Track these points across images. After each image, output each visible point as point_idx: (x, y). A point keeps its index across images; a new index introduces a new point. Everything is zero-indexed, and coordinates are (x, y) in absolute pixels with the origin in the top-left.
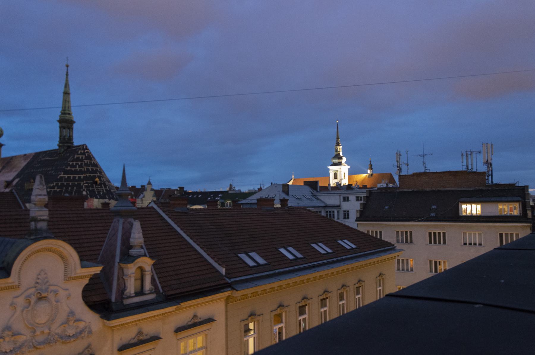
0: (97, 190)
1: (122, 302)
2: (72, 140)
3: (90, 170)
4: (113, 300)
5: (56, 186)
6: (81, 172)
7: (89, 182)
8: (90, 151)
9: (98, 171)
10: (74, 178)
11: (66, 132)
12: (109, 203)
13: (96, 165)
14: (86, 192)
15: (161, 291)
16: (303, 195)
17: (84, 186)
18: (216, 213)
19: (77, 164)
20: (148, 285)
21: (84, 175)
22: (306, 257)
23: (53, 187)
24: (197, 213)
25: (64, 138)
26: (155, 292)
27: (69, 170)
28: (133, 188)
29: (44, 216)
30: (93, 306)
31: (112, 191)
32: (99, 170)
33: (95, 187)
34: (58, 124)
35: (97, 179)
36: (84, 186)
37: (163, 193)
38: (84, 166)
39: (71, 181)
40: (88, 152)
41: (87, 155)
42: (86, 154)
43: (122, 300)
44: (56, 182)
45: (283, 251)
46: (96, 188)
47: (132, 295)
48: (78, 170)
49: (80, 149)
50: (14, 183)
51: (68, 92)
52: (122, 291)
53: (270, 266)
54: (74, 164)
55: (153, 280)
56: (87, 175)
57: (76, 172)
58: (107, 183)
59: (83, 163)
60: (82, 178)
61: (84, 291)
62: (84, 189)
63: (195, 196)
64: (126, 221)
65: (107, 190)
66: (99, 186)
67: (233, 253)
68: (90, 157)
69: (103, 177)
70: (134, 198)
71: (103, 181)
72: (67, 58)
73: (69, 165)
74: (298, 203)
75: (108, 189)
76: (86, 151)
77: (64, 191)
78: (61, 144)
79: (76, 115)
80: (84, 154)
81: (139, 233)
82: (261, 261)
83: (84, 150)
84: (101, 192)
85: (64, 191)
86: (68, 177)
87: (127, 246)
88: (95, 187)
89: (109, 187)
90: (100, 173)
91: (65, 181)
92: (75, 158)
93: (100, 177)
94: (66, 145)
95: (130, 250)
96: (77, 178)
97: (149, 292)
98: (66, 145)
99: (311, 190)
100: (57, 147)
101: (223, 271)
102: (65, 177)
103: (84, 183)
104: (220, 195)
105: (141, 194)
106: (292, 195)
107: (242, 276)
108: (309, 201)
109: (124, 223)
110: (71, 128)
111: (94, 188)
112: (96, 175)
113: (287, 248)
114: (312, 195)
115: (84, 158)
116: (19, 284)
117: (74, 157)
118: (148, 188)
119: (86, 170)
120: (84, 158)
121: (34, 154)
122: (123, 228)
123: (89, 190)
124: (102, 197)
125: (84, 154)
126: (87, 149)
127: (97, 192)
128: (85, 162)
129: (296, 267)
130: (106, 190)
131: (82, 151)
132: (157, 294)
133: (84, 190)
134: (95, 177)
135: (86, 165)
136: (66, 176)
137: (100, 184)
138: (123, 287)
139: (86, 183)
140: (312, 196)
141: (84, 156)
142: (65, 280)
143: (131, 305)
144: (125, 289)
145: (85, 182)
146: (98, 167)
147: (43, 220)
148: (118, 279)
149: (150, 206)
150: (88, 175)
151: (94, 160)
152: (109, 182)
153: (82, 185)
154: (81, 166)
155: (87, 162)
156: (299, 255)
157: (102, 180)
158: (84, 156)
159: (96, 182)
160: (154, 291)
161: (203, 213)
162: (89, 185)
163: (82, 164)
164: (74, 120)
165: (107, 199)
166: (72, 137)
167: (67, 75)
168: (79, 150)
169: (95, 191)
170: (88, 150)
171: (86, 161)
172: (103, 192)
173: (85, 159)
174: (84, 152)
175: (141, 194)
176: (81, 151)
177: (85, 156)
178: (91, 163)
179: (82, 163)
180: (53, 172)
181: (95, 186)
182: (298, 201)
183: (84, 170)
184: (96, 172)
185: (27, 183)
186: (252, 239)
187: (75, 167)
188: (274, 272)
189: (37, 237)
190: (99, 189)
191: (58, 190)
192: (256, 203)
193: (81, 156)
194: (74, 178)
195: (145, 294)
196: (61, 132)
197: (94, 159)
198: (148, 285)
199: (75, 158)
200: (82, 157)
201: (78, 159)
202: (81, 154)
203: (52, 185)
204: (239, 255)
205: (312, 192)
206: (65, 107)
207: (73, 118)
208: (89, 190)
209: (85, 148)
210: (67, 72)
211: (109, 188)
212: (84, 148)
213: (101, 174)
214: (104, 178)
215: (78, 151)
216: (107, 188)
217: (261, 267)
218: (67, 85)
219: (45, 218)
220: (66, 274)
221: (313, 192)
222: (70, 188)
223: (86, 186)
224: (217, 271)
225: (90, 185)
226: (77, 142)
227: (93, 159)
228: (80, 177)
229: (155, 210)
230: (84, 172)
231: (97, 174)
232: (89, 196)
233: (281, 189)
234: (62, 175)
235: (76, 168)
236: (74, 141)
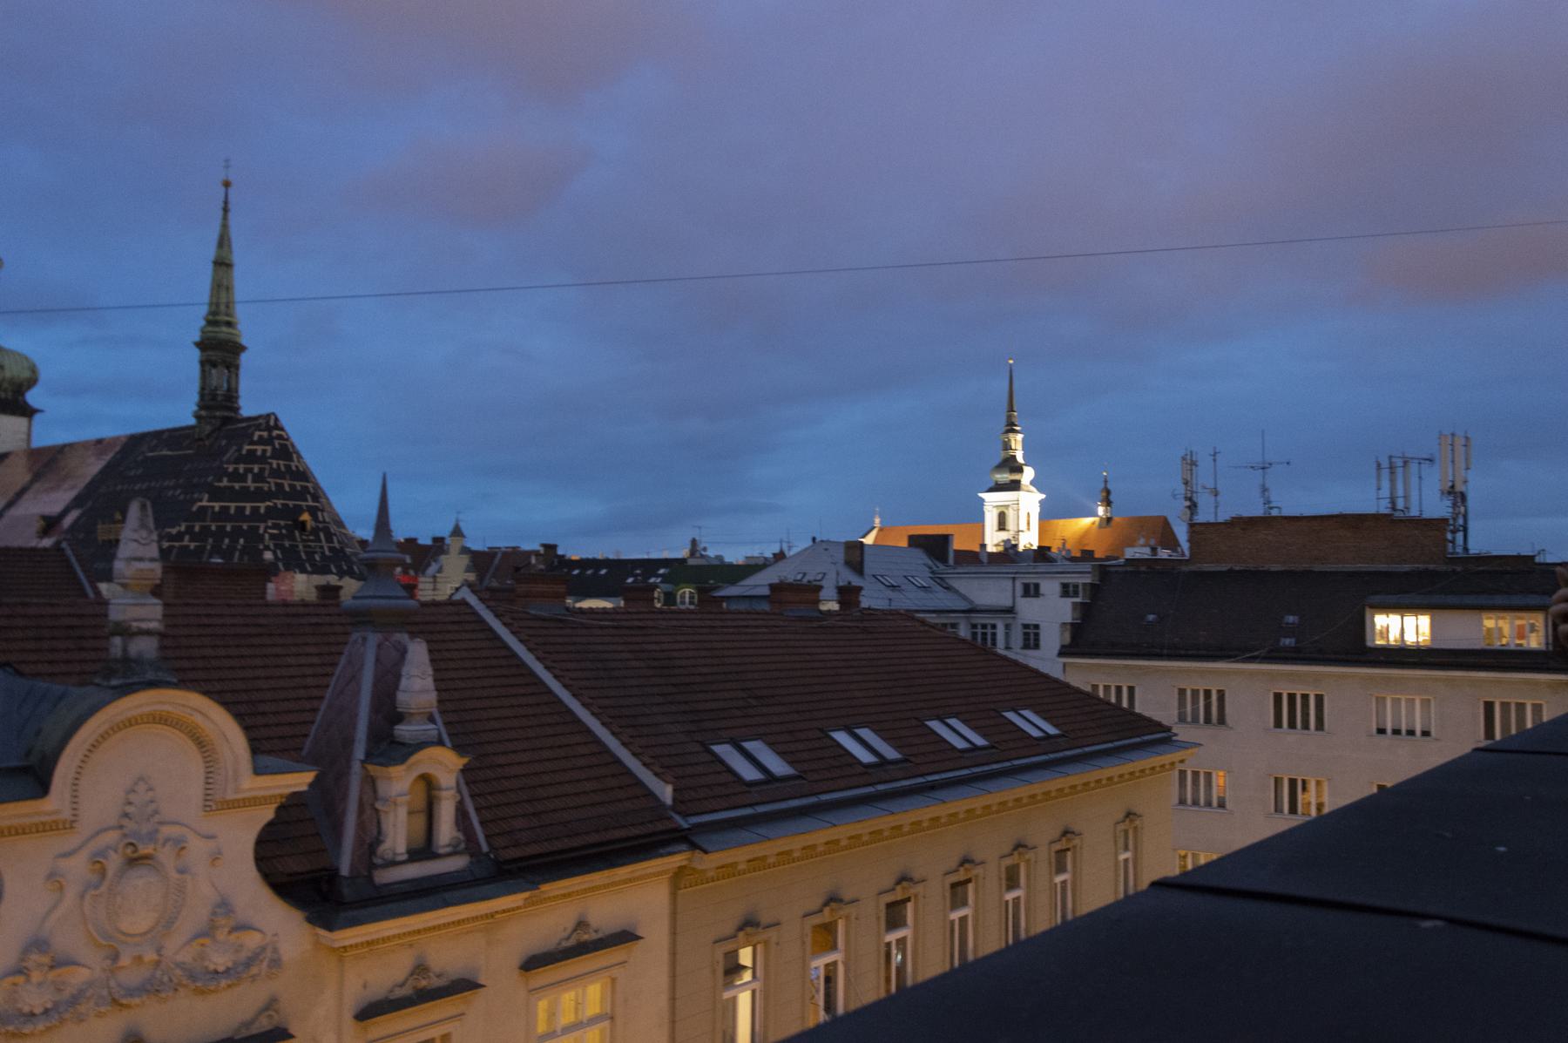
0: (305, 547)
1: (370, 878)
2: (236, 402)
3: (287, 489)
4: (345, 870)
6: (260, 495)
7: (282, 523)
8: (287, 434)
9: (309, 493)
10: (241, 510)
11: (218, 377)
12: (340, 588)
13: (304, 475)
15: (485, 848)
16: (905, 577)
17: (267, 536)
18: (650, 623)
20: (446, 831)
21: (268, 503)
22: (912, 759)
23: (179, 537)
24: (595, 622)
25: (214, 397)
26: (467, 851)
27: (225, 487)
28: (411, 542)
29: (150, 620)
30: (285, 887)
31: (348, 550)
32: (312, 490)
33: (299, 540)
34: (196, 354)
35: (305, 517)
36: (267, 536)
37: (496, 561)
38: (269, 477)
39: (230, 518)
40: (280, 437)
41: (277, 446)
42: (277, 443)
44: (186, 521)
45: (842, 738)
48: (252, 489)
49: (258, 428)
50: (68, 521)
51: (227, 261)
52: (370, 844)
53: (804, 782)
54: (241, 471)
55: (461, 816)
56: (275, 504)
57: (245, 495)
58: (333, 528)
59: (267, 467)
60: (262, 511)
62: (266, 543)
63: (589, 572)
64: (387, 640)
65: (335, 547)
66: (311, 538)
67: (697, 742)
68: (286, 451)
69: (322, 511)
70: (412, 573)
71: (324, 522)
72: (227, 161)
73: (226, 473)
75: (336, 545)
76: (275, 433)
77: (209, 547)
78: (203, 413)
79: (248, 327)
80: (269, 441)
82: (778, 766)
84: (316, 552)
85: (209, 547)
86: (221, 507)
87: (388, 713)
88: (299, 540)
89: (340, 539)
90: (316, 498)
91: (213, 520)
92: (244, 452)
93: (313, 512)
94: (218, 414)
95: (396, 727)
96: (248, 512)
97: (448, 850)
98: (218, 414)
99: (930, 563)
100: (192, 421)
101: (666, 793)
102: (213, 507)
103: (267, 527)
104: (662, 571)
105: (433, 564)
106: (874, 576)
107: (721, 810)
108: (922, 594)
109: (379, 646)
110: (232, 367)
111: (296, 541)
112: (304, 503)
114: (931, 575)
115: (268, 454)
116: (73, 818)
117: (240, 450)
118: (454, 545)
119: (273, 489)
120: (268, 454)
121: (124, 440)
122: (378, 660)
123: (281, 547)
124: (324, 570)
126: (278, 426)
127: (306, 553)
128: (271, 464)
129: (881, 787)
130: (331, 549)
131: (265, 434)
134: (299, 510)
135: (276, 473)
136: (217, 506)
137: (315, 531)
138: (375, 832)
139: (275, 526)
140: (931, 578)
141: (269, 448)
142: (208, 809)
143: (396, 886)
145: (270, 524)
146: (308, 482)
147: (148, 633)
148: (361, 810)
149: (457, 597)
150: (279, 503)
151: (299, 462)
152: (340, 524)
153: (261, 531)
154: (259, 478)
155: (278, 465)
156: (890, 753)
157: (321, 519)
159: (303, 524)
160: (463, 846)
163: (262, 470)
164: (244, 341)
165: (332, 573)
166: (237, 392)
167: (226, 210)
168: (256, 430)
169: (299, 552)
170: (282, 429)
171: (274, 463)
172: (323, 553)
173: (272, 457)
174: (270, 435)
175: (433, 564)
176: (262, 433)
177: (274, 449)
178: (288, 467)
179: (264, 469)
180: (178, 491)
181: (301, 535)
182: (891, 593)
183: (270, 488)
184: (302, 494)
185: (104, 523)
186: (754, 702)
187: (243, 478)
188: (816, 799)
189: (130, 681)
190: (313, 544)
191: (192, 545)
192: (768, 596)
193: (259, 449)
194: (241, 510)
195: (435, 856)
196: (204, 375)
197: (299, 457)
198: (446, 831)
199: (244, 452)
200: (264, 451)
201: (251, 457)
202: (261, 441)
203: (174, 531)
204: (717, 749)
205: (930, 568)
206: (218, 305)
207: (239, 336)
208: (281, 547)
209: (272, 423)
210: (226, 202)
211: (339, 542)
212: (269, 424)
213: (318, 502)
214: (325, 514)
215: (253, 434)
216: (332, 542)
217: (778, 785)
218: (224, 241)
219: (153, 625)
220: (209, 792)
221: (935, 568)
222: (227, 541)
223: (272, 537)
224: (649, 794)
225: (284, 531)
226: (249, 407)
227: (295, 456)
228: (255, 510)
229: (469, 611)
230: (268, 496)
231: (306, 500)
232: (280, 565)
233: (840, 556)
234: (204, 503)
235: (246, 482)
236: (242, 402)
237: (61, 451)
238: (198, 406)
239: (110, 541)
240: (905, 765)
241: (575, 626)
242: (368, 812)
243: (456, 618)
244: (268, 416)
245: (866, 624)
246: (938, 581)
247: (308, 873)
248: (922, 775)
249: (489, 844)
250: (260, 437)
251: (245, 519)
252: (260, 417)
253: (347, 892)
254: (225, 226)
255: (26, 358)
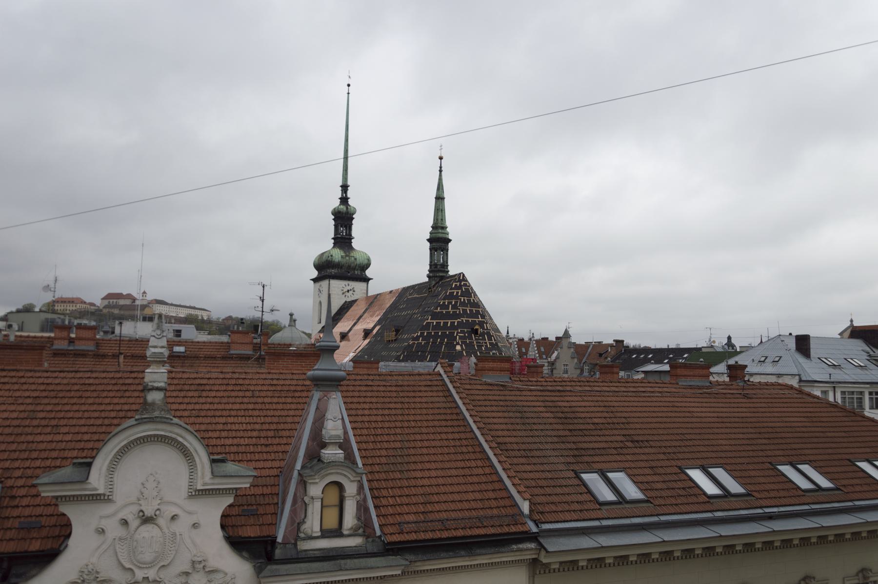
1: (295, 545)
5: (420, 336)
6: (455, 316)
7: (466, 330)
8: (469, 283)
9: (480, 314)
13: (477, 305)
14: (461, 346)
15: (378, 533)
16: (845, 359)
18: (568, 388)
19: (450, 303)
22: (754, 494)
23: (417, 338)
29: (159, 382)
30: (237, 543)
35: (477, 327)
43: (296, 540)
45: (787, 470)
46: (476, 339)
47: (315, 535)
52: (297, 524)
53: (753, 498)
55: (362, 508)
56: (462, 320)
57: (448, 316)
58: (492, 332)
61: (224, 516)
63: (642, 356)
64: (326, 396)
66: (481, 338)
67: (572, 470)
68: (468, 292)
69: (487, 323)
71: (487, 329)
73: (439, 305)
74: (830, 374)
80: (460, 287)
81: (335, 420)
82: (632, 491)
83: (460, 281)
84: (483, 346)
87: (318, 442)
90: (483, 317)
95: (323, 451)
97: (351, 532)
99: (868, 349)
100: (427, 280)
101: (525, 507)
103: (458, 333)
104: (685, 356)
105: (556, 352)
106: (819, 358)
107: (571, 521)
108: (859, 371)
109: (319, 400)
110: (445, 250)
113: (798, 466)
114: (868, 358)
121: (400, 291)
122: (317, 408)
123: (465, 343)
125: (460, 287)
126: (464, 279)
128: (461, 299)
129: (719, 514)
131: (458, 284)
132: (368, 537)
133: (458, 344)
135: (463, 304)
137: (483, 334)
140: (868, 360)
141: (460, 291)
142: (190, 494)
143: (311, 552)
144: (305, 520)
147: (158, 389)
149: (436, 370)
150: (464, 319)
155: (464, 300)
156: (735, 487)
158: (460, 291)
159: (477, 330)
160: (361, 531)
161: (538, 388)
162: (465, 335)
163: (456, 303)
168: (454, 282)
170: (467, 281)
172: (486, 346)
173: (461, 296)
174: (460, 285)
175: (556, 352)
181: (475, 336)
182: (833, 370)
183: (460, 312)
186: (629, 444)
188: (658, 519)
190: (481, 341)
192: (669, 371)
197: (475, 295)
198: (350, 520)
200: (457, 293)
202: (456, 288)
204: (585, 476)
205: (868, 353)
212: (461, 278)
217: (627, 506)
218: (440, 187)
219: (162, 385)
220: (111, 487)
221: (872, 353)
224: (516, 505)
225: (467, 335)
228: (453, 323)
229: (441, 378)
233: (792, 344)
234: (429, 321)
237: (376, 297)
238: (429, 271)
239: (389, 341)
240: (836, 492)
241: (512, 389)
242: (299, 503)
243: (429, 383)
244: (460, 274)
245: (745, 392)
246: (874, 362)
247: (254, 538)
248: (761, 507)
249: (381, 530)
250: (456, 285)
251: (449, 328)
252: (456, 275)
253: (278, 553)
254: (440, 179)
255: (366, 254)
